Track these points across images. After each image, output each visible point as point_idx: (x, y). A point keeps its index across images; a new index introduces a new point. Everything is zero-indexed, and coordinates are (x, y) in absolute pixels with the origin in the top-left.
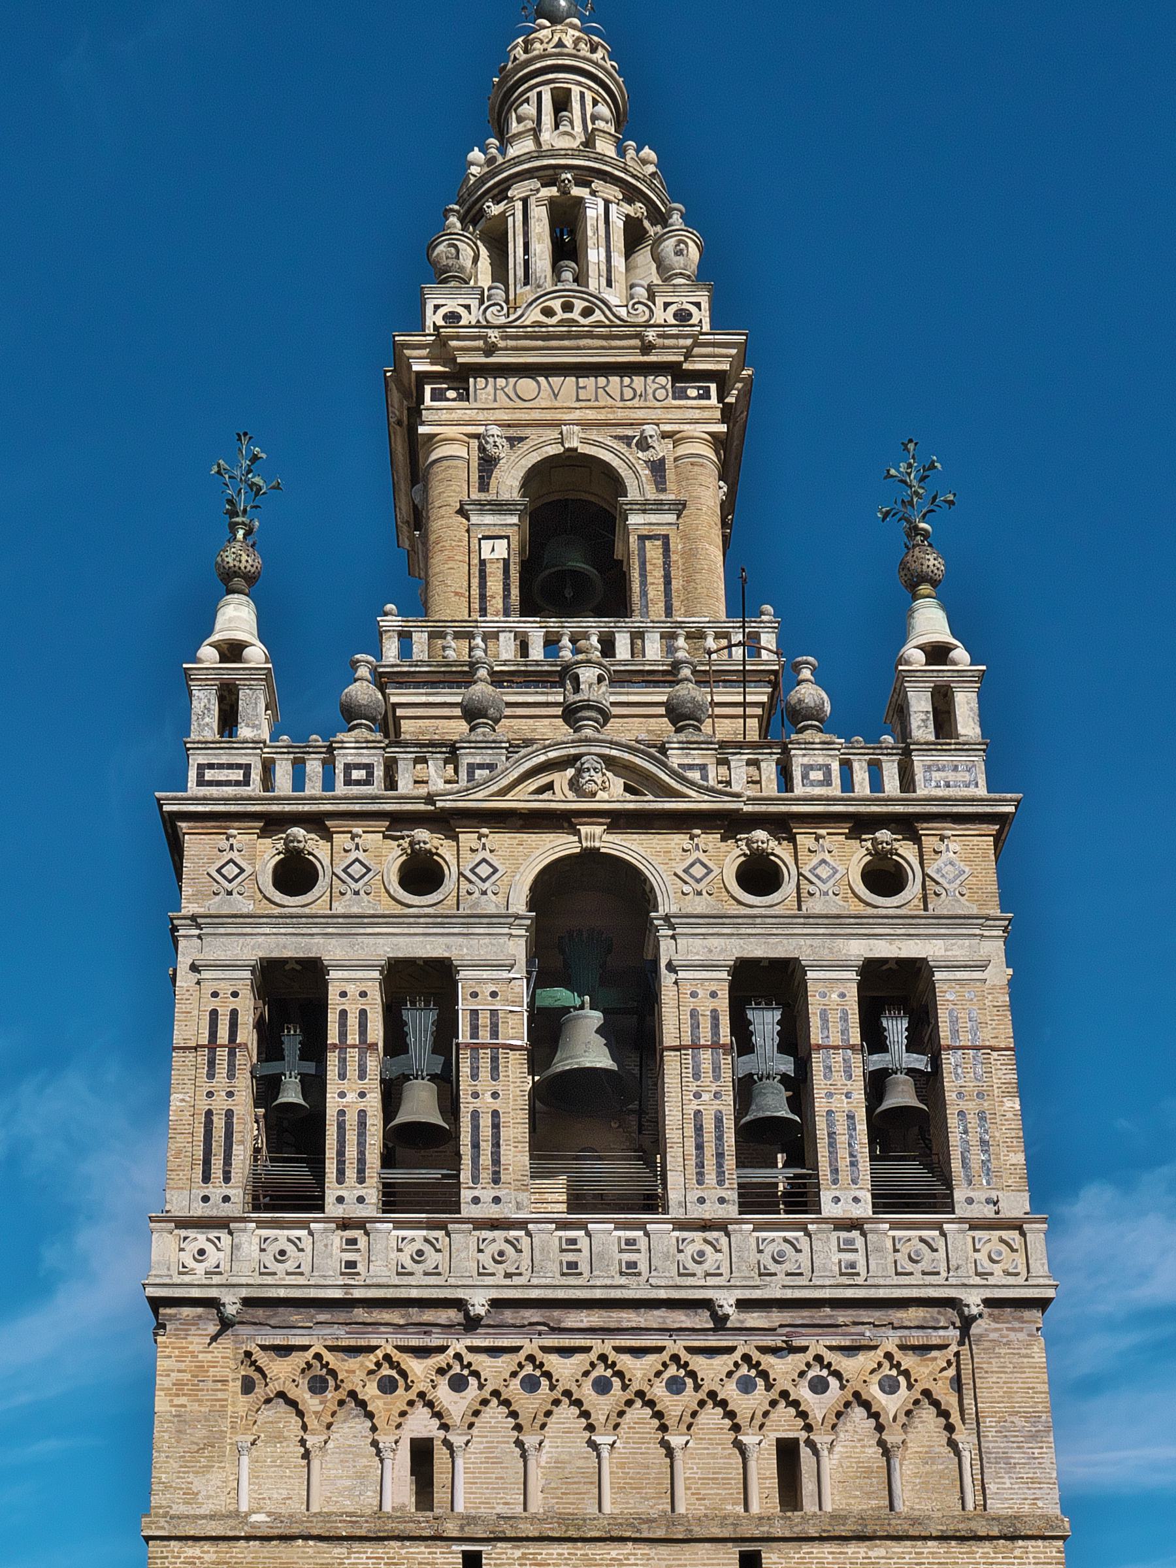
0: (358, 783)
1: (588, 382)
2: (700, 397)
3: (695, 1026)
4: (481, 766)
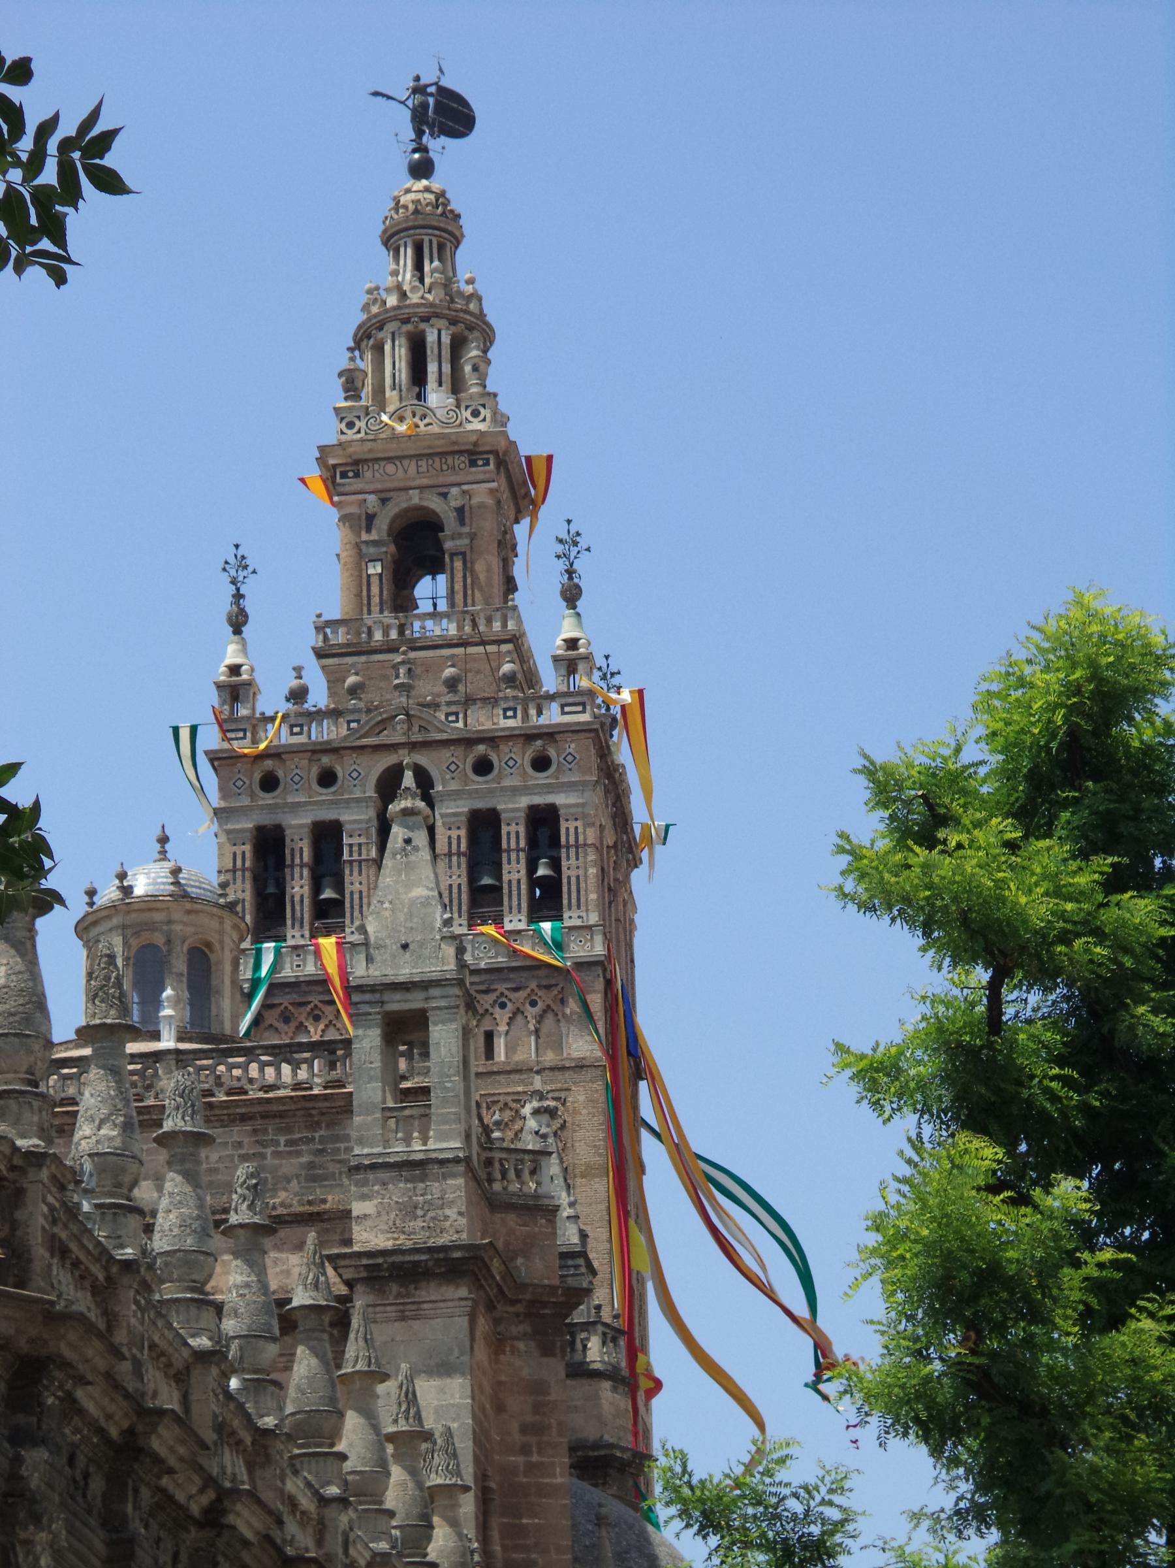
0: (296, 734)
1: (423, 463)
2: (484, 465)
3: (450, 843)
4: (353, 721)
